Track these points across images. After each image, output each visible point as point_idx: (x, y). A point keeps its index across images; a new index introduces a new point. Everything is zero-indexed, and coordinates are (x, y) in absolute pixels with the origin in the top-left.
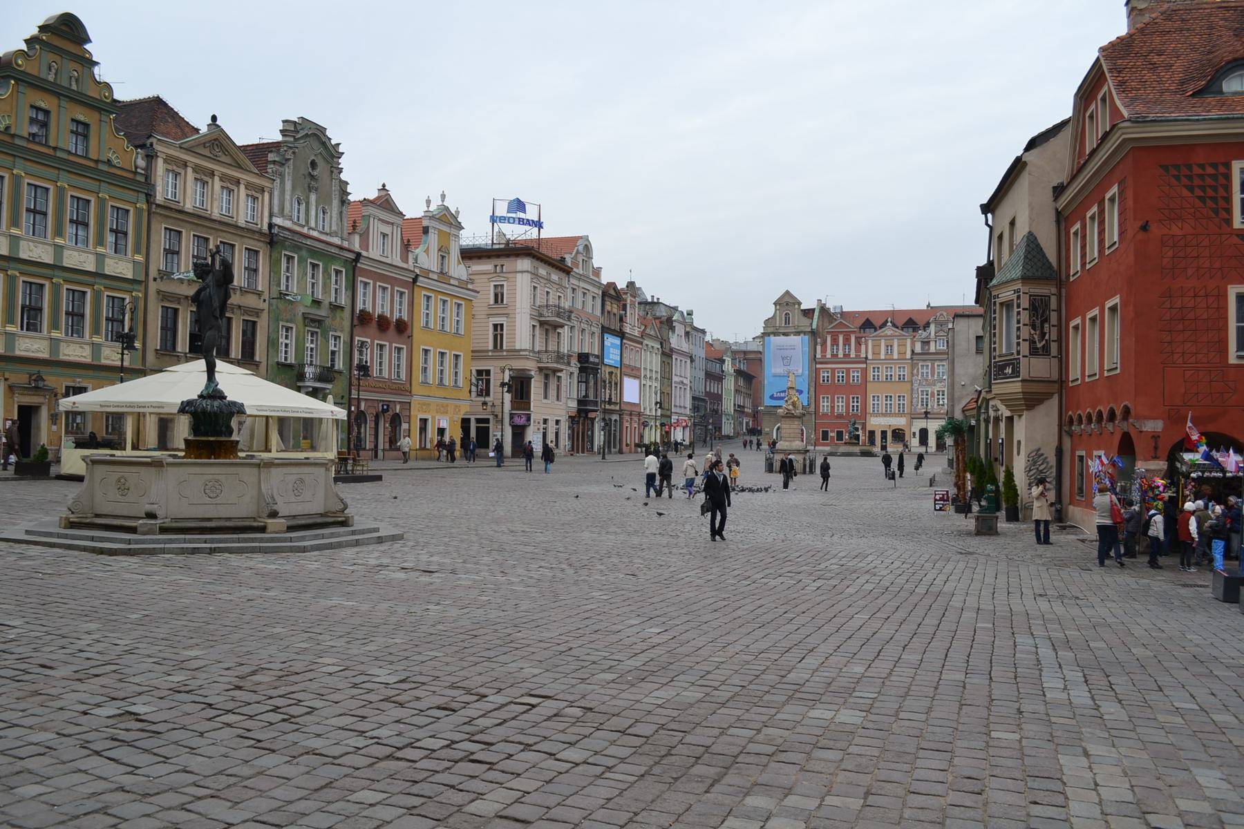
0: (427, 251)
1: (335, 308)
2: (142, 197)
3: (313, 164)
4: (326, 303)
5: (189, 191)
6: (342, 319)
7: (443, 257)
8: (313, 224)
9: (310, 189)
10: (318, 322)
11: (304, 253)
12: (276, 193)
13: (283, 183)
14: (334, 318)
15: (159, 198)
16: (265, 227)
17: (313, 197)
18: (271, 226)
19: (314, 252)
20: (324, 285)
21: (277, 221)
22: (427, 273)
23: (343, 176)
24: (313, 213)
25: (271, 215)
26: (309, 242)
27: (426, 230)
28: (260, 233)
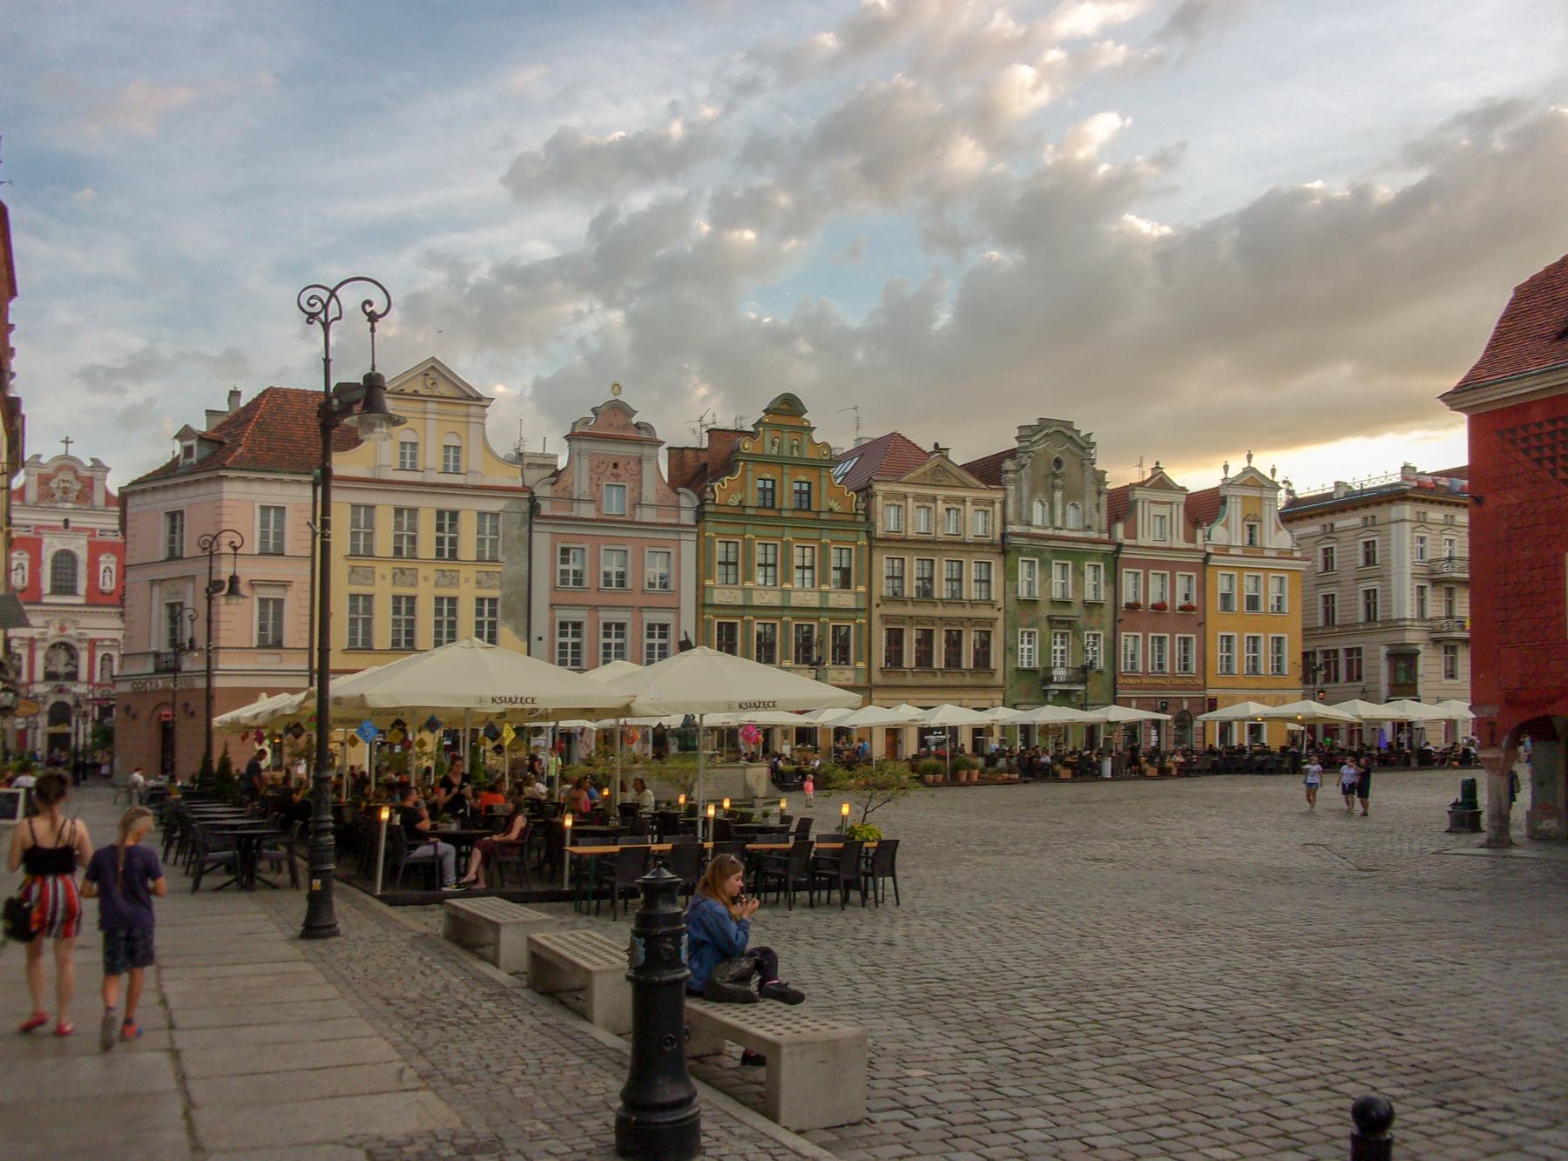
0: (1226, 525)
1: (1090, 606)
2: (863, 535)
3: (1058, 462)
4: (1078, 601)
5: (910, 521)
6: (1101, 616)
7: (1251, 528)
8: (1059, 523)
9: (1054, 487)
10: (1069, 623)
11: (1047, 555)
12: (1010, 502)
13: (1018, 490)
14: (1090, 616)
15: (879, 533)
16: (998, 538)
17: (1058, 495)
18: (1004, 536)
19: (1059, 553)
20: (1076, 584)
21: (1010, 529)
22: (1224, 550)
23: (1098, 467)
24: (1059, 512)
25: (1004, 523)
26: (1052, 543)
27: (1224, 501)
28: (991, 545)
